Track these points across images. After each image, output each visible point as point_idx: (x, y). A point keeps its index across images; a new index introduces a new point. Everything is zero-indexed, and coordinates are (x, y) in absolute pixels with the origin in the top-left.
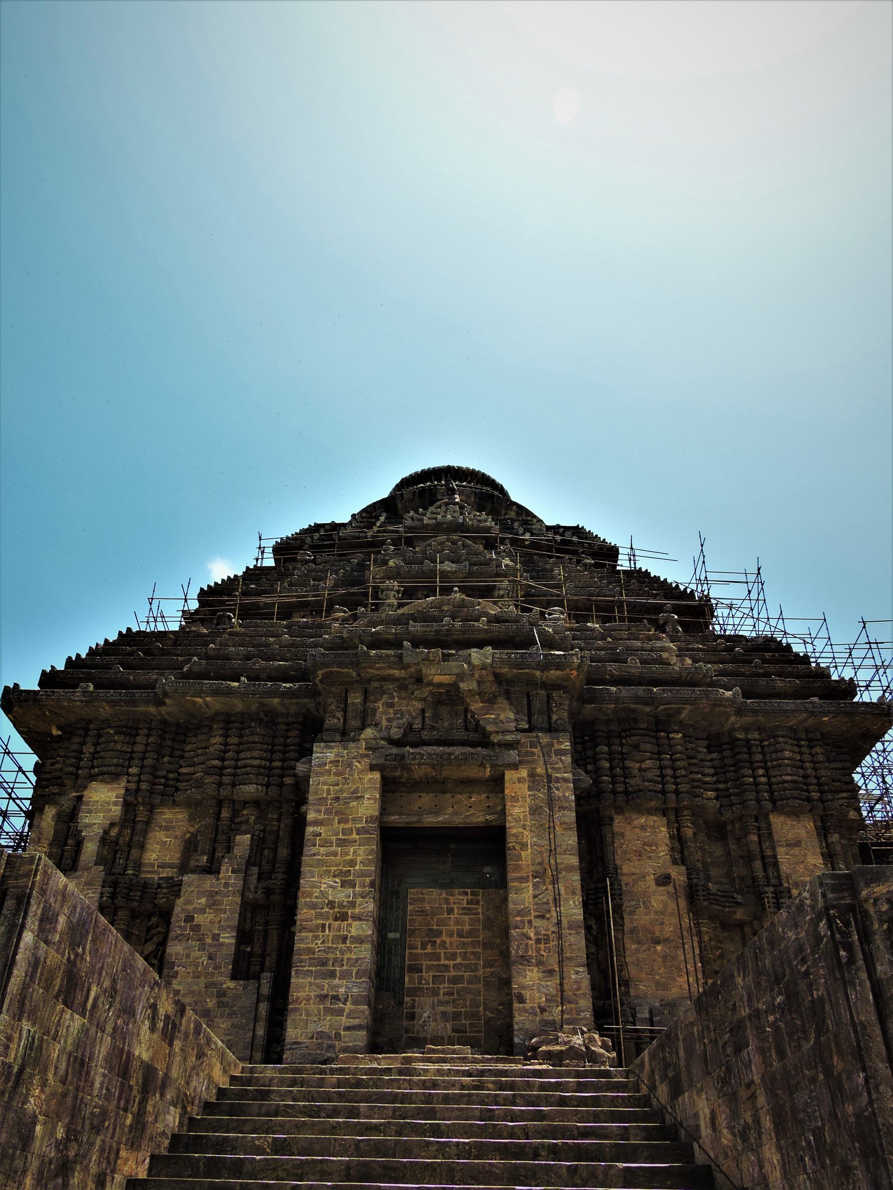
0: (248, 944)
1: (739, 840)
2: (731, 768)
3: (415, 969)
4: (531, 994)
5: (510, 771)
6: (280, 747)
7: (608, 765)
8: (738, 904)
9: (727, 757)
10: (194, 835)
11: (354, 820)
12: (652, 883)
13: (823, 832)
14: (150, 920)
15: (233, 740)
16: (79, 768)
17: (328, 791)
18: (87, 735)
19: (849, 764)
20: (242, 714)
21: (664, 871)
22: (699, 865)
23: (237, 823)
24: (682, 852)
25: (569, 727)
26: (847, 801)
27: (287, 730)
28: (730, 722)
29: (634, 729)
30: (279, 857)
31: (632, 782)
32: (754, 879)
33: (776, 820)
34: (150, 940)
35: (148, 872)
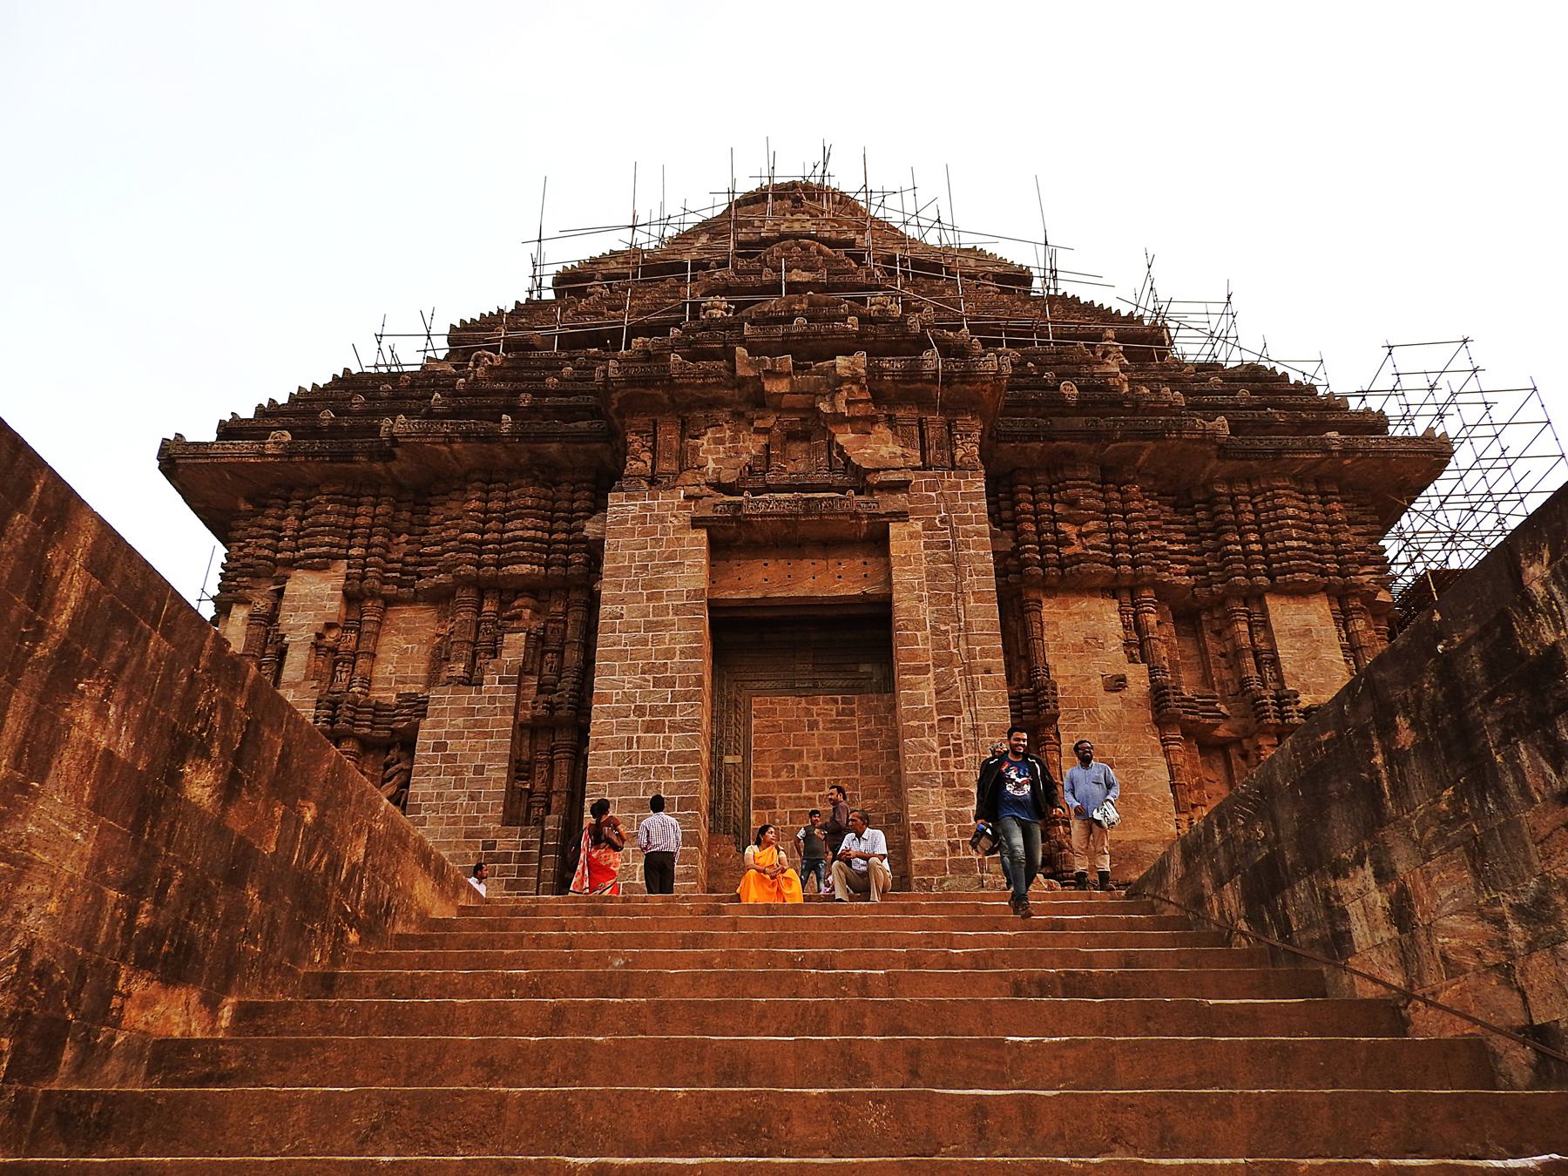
0: (527, 779)
1: (1218, 633)
2: (1209, 535)
4: (936, 825)
5: (896, 524)
6: (562, 514)
8: (1224, 717)
9: (1202, 520)
13: (1343, 618)
15: (494, 505)
16: (277, 551)
19: (1379, 528)
21: (1115, 672)
23: (505, 619)
24: (1141, 646)
26: (1376, 576)
27: (573, 492)
28: (1208, 469)
29: (1070, 480)
30: (566, 664)
32: (1243, 683)
34: (390, 779)
35: (383, 689)
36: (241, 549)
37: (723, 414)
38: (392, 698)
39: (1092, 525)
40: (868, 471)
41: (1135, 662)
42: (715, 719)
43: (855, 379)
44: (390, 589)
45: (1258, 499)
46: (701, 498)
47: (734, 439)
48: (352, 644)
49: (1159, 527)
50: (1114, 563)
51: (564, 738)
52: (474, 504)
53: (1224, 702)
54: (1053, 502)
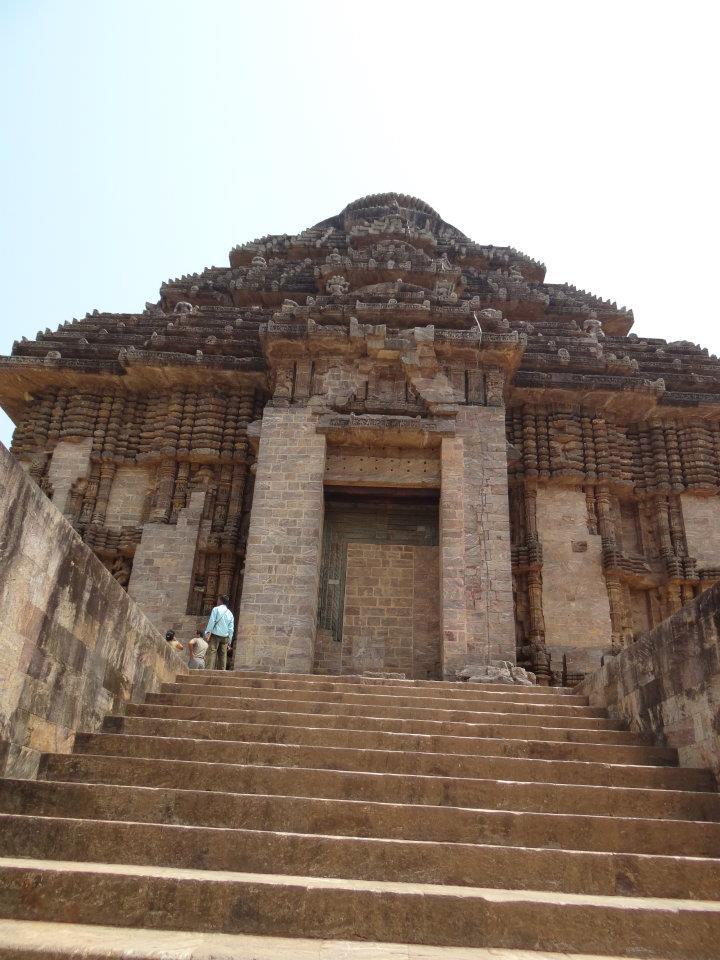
0: (202, 586)
1: (649, 518)
3: (353, 611)
7: (535, 444)
10: (154, 492)
12: (570, 552)
14: (114, 563)
15: (187, 408)
16: (48, 429)
18: (56, 401)
20: (199, 386)
22: (613, 536)
24: (598, 524)
30: (230, 513)
31: (556, 460)
32: (662, 551)
35: (113, 522)
36: (25, 426)
37: (338, 359)
38: (118, 528)
39: (572, 445)
41: (593, 534)
42: (325, 555)
44: (120, 459)
45: (680, 433)
46: (323, 414)
49: (615, 448)
51: (227, 563)
53: (649, 562)
54: (548, 428)
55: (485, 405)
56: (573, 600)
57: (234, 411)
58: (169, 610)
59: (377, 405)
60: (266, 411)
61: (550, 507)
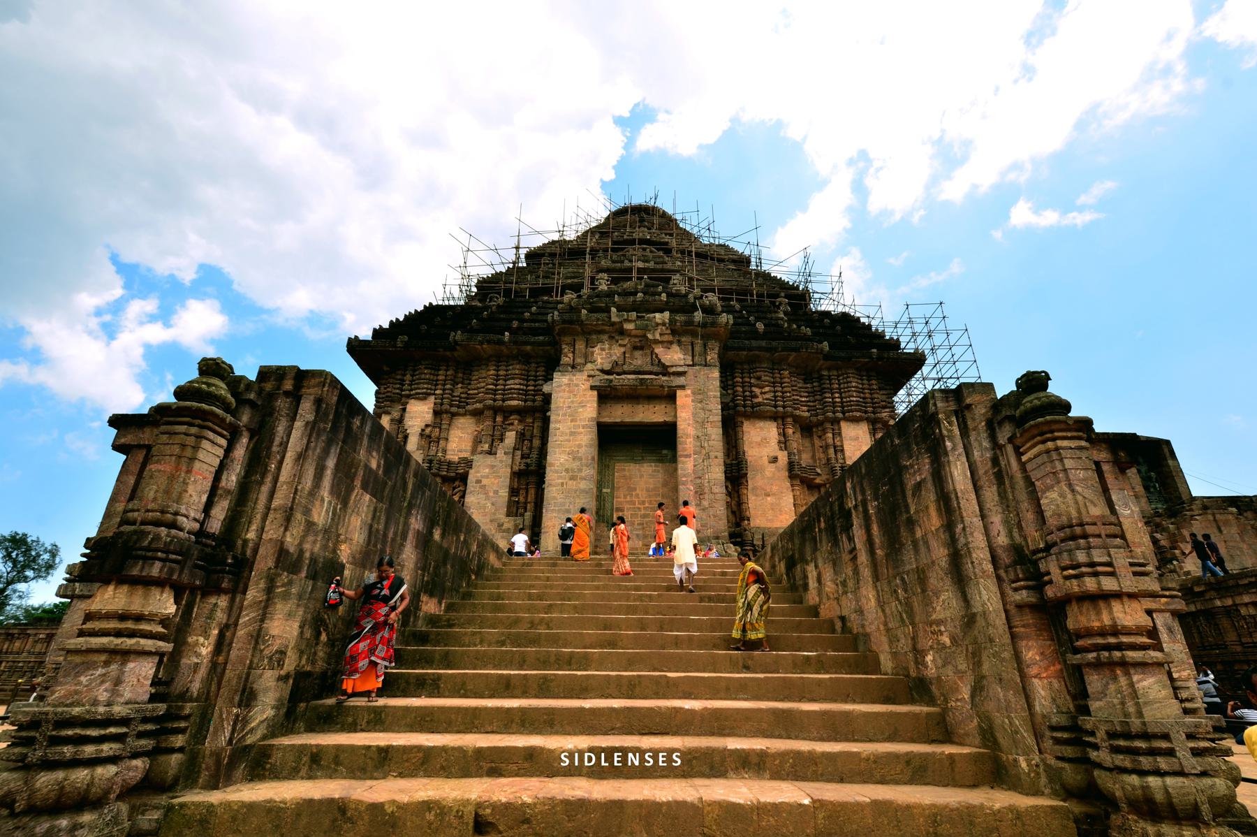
1: (820, 437)
11: (580, 420)
15: (501, 373)
16: (402, 390)
17: (564, 402)
19: (892, 392)
21: (772, 454)
22: (795, 451)
24: (785, 443)
25: (718, 364)
30: (534, 445)
31: (756, 400)
32: (829, 460)
33: (843, 424)
36: (385, 389)
37: (605, 337)
38: (456, 459)
39: (767, 389)
40: (668, 366)
42: (600, 472)
43: (664, 324)
44: (454, 409)
47: (610, 349)
48: (437, 434)
49: (796, 390)
50: (776, 406)
51: (532, 479)
52: (492, 372)
53: (820, 468)
54: (751, 378)
55: (706, 366)
56: (769, 496)
57: (533, 373)
58: (494, 514)
59: (632, 368)
60: (556, 375)
61: (753, 433)
